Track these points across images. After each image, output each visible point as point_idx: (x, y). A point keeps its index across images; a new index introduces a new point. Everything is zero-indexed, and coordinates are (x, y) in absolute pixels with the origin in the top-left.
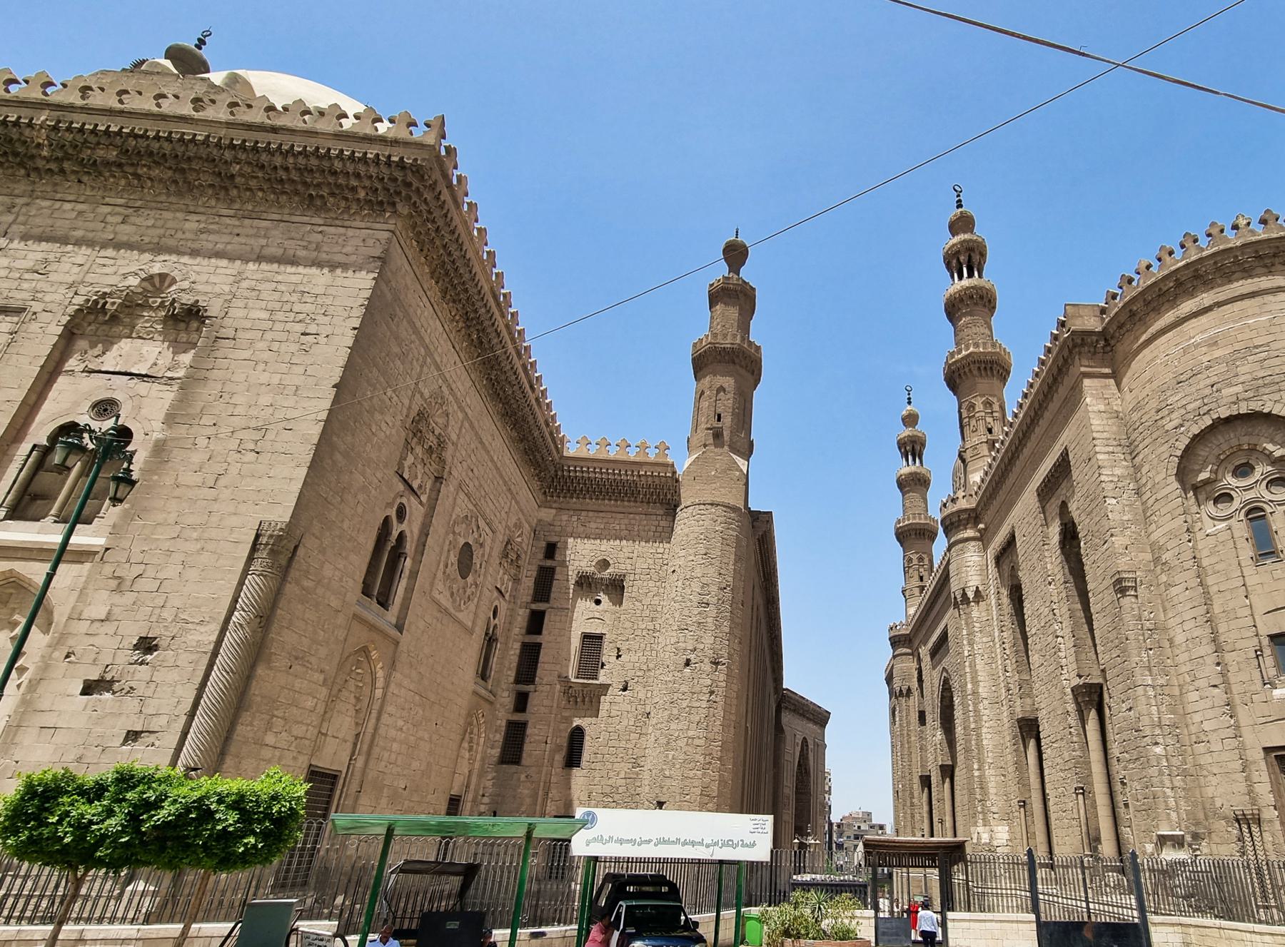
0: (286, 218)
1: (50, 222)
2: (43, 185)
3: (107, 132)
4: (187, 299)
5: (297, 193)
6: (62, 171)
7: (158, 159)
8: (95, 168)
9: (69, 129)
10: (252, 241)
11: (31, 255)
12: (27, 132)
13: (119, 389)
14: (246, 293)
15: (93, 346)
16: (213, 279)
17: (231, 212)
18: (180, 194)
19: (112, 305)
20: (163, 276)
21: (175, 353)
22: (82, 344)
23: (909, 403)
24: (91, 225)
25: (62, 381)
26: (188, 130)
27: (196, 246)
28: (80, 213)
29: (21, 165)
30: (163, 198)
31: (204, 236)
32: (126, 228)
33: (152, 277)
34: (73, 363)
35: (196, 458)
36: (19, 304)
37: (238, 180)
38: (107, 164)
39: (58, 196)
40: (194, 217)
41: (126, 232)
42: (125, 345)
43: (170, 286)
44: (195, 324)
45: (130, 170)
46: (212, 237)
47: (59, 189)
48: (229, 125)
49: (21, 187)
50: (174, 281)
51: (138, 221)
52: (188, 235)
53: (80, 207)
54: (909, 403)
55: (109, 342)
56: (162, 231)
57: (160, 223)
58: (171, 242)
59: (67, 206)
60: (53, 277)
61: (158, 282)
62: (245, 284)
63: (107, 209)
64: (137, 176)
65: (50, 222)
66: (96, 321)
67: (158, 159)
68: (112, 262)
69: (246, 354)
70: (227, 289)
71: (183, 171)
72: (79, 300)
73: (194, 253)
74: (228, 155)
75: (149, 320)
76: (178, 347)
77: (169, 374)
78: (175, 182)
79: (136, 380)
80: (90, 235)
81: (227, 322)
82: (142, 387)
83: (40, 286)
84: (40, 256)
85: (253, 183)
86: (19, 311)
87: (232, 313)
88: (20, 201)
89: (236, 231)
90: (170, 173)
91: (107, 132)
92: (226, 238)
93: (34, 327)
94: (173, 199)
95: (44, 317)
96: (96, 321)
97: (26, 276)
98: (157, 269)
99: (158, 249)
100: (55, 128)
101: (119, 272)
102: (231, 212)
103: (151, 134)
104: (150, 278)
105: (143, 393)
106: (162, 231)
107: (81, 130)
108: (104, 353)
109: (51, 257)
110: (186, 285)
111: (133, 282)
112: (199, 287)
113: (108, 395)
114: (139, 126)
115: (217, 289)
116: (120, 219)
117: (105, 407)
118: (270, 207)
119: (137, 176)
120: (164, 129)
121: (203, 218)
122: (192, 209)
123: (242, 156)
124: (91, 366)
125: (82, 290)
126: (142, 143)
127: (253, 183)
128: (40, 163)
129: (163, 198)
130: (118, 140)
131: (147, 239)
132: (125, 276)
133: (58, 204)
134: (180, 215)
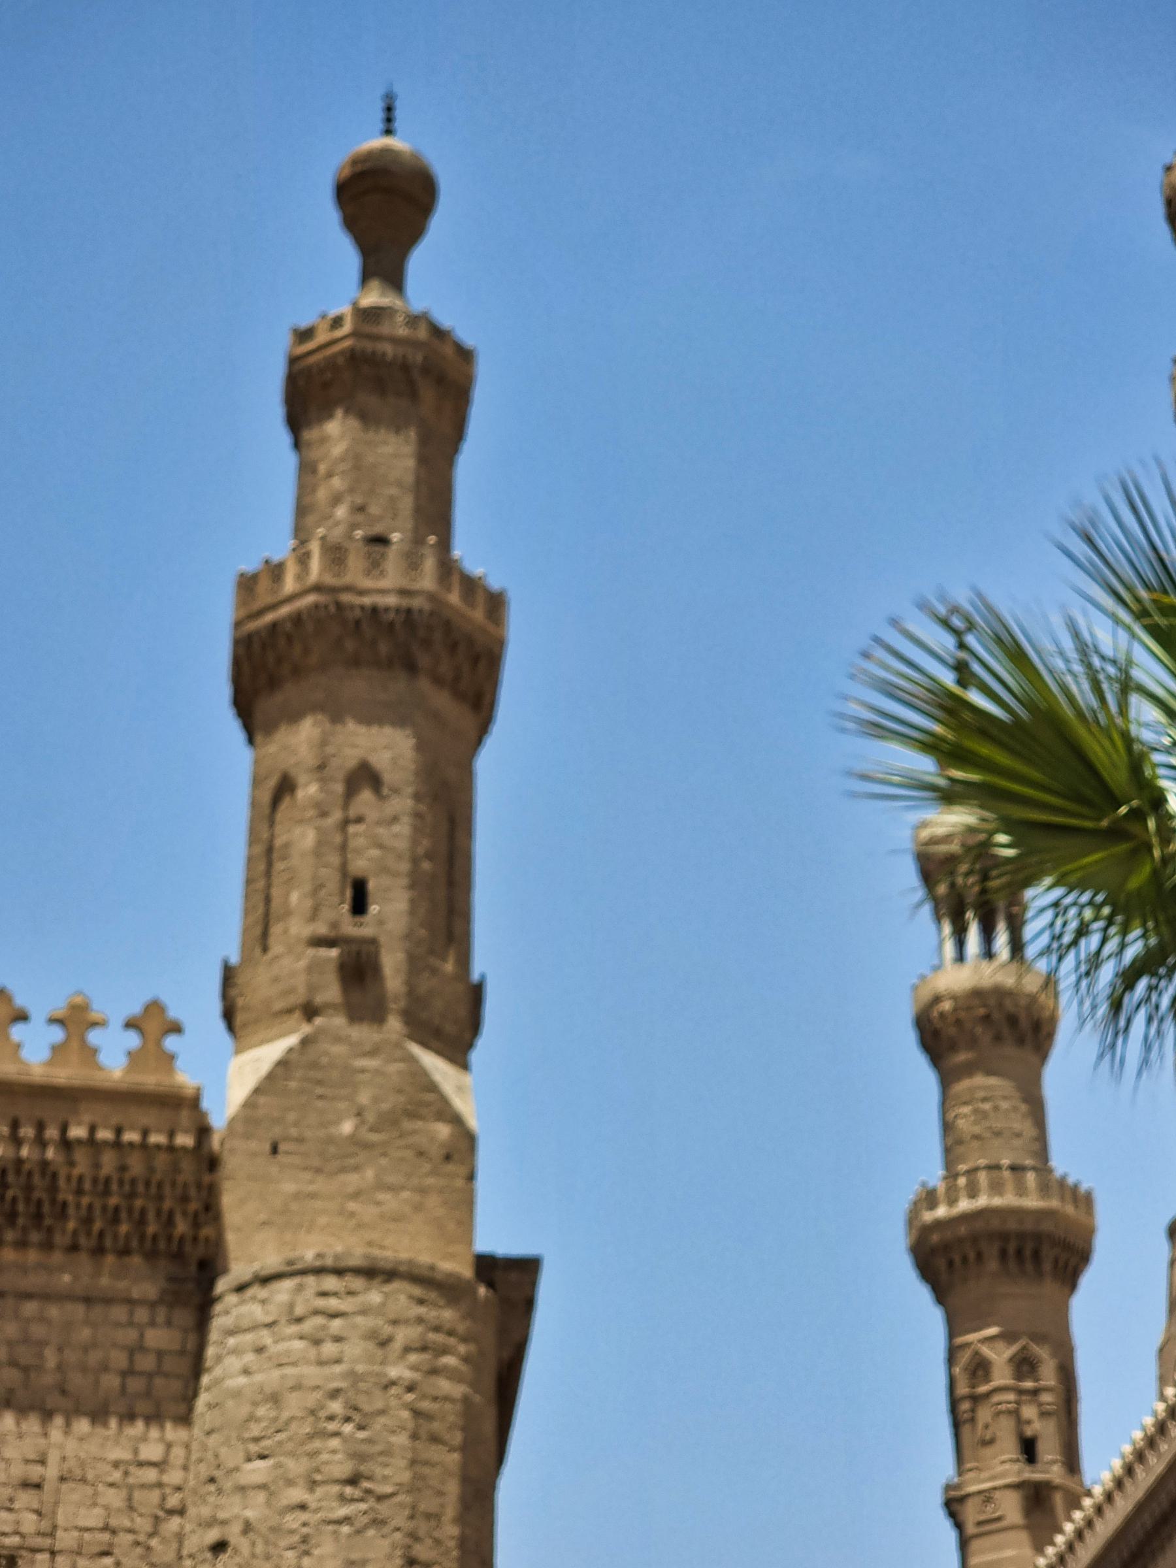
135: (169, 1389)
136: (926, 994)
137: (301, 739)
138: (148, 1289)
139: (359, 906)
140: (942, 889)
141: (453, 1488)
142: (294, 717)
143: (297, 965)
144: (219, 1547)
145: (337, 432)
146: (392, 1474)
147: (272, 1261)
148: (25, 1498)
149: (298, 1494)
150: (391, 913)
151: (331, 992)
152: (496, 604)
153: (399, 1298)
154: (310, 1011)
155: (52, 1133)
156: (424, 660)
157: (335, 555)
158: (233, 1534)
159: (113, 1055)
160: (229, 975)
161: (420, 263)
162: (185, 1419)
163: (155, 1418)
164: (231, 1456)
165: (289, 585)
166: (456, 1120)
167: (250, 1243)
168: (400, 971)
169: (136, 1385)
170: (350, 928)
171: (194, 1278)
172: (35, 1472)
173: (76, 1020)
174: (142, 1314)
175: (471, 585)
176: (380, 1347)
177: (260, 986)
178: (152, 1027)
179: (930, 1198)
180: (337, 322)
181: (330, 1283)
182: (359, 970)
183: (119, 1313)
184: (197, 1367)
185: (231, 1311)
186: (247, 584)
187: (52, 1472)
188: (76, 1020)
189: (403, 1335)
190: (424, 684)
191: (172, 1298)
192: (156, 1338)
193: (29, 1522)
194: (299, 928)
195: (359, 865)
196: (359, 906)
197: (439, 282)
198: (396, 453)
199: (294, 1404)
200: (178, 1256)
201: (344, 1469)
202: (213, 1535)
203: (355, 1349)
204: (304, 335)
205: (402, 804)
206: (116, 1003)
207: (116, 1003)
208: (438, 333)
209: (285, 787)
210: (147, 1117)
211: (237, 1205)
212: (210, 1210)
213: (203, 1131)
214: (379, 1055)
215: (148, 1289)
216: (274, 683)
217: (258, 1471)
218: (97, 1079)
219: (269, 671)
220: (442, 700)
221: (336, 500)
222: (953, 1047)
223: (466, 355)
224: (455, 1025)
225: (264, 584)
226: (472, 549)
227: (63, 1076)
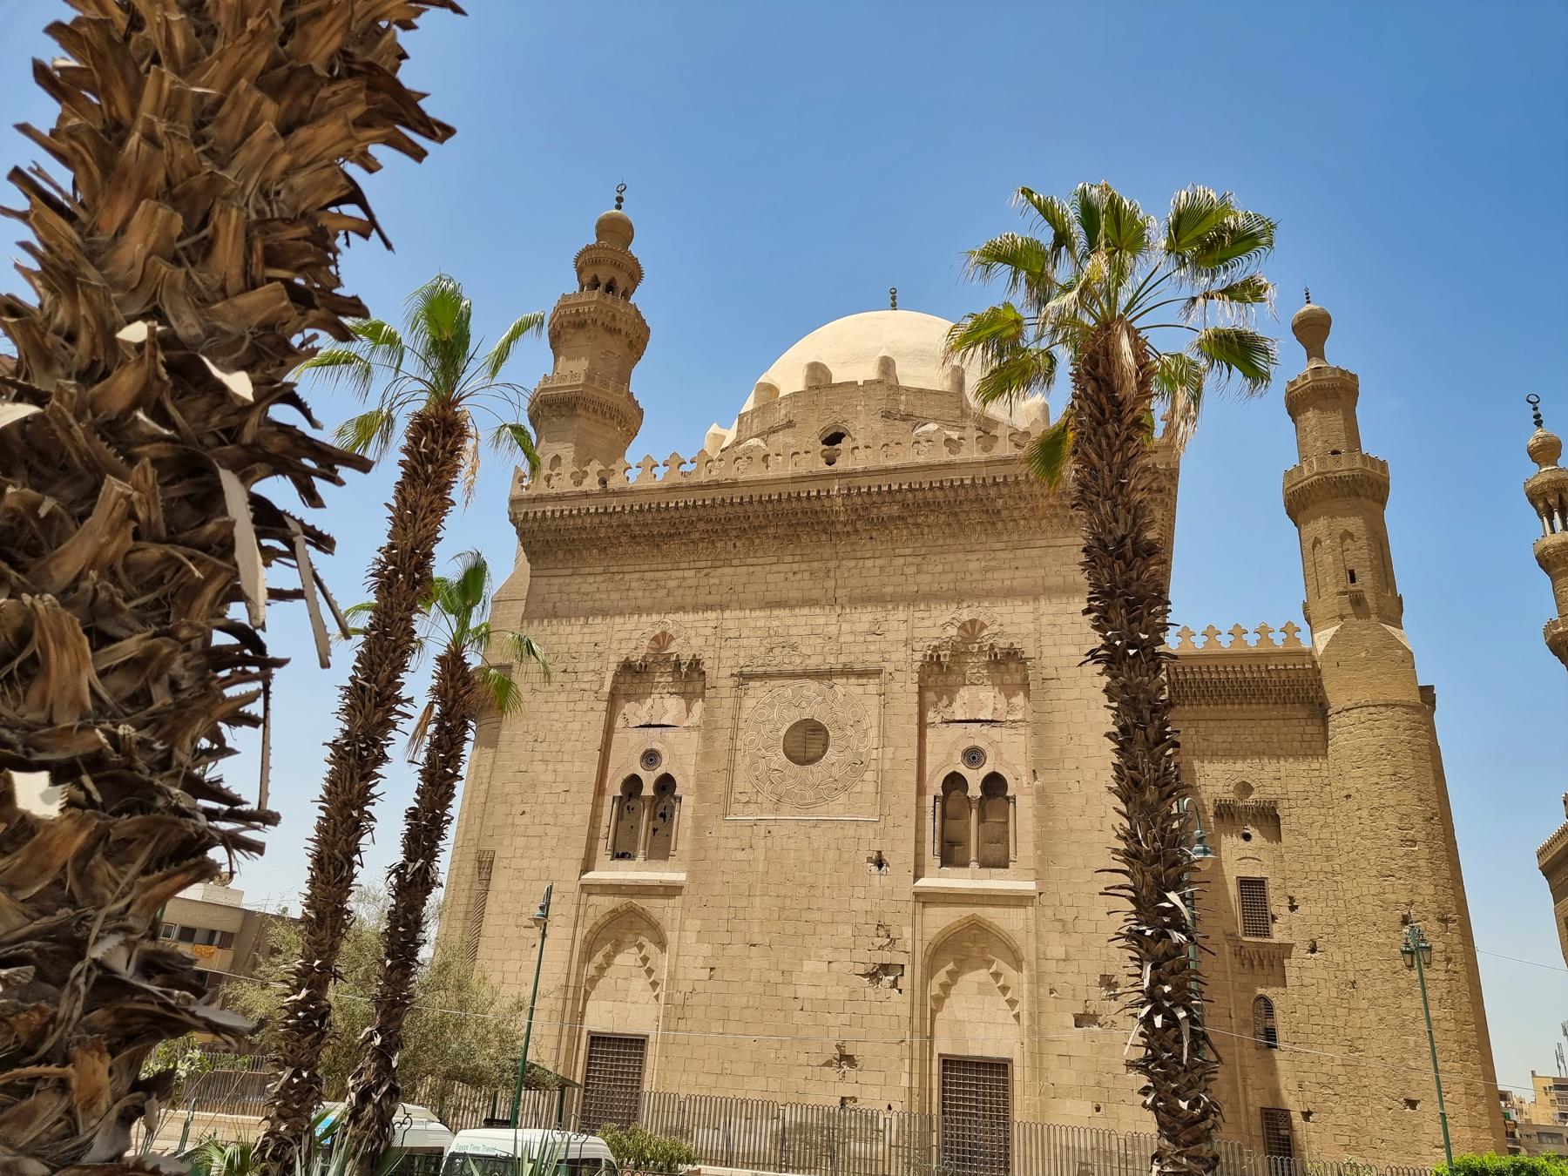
0: (1052, 542)
1: (862, 581)
2: (841, 548)
3: (890, 491)
4: (1003, 643)
5: (1056, 515)
6: (856, 531)
7: (932, 507)
8: (882, 523)
9: (859, 494)
10: (1031, 573)
11: (863, 618)
12: (827, 502)
13: (978, 736)
14: (1050, 629)
15: (940, 699)
16: (1016, 619)
17: (1002, 545)
18: (954, 535)
19: (945, 655)
20: (973, 622)
21: (1008, 697)
22: (930, 696)
23: (1539, 423)
24: (895, 579)
25: (929, 732)
26: (955, 476)
27: (987, 586)
28: (882, 568)
29: (825, 531)
30: (941, 542)
31: (989, 575)
32: (924, 578)
33: (964, 624)
34: (931, 716)
35: (1076, 802)
36: (873, 667)
37: (1005, 513)
38: (892, 518)
39: (858, 555)
40: (974, 557)
41: (925, 582)
42: (964, 694)
43: (981, 630)
44: (1013, 665)
45: (910, 520)
46: (996, 575)
47: (857, 547)
48: (988, 463)
49: (827, 551)
50: (983, 626)
51: (930, 568)
52: (977, 576)
53: (879, 562)
54: (1539, 423)
55: (949, 692)
56: (951, 576)
57: (948, 567)
58: (966, 586)
59: (869, 563)
60: (889, 636)
61: (971, 629)
62: (1044, 620)
63: (901, 561)
64: (917, 525)
65: (862, 581)
66: (938, 674)
67: (932, 507)
68: (926, 614)
69: (1074, 693)
70: (1031, 627)
71: (956, 514)
72: (918, 656)
73: (990, 594)
74: (993, 492)
75: (974, 666)
76: (1008, 691)
77: (1010, 718)
78: (949, 525)
79: (986, 727)
80: (899, 589)
81: (1045, 662)
82: (995, 733)
83: (883, 646)
84: (870, 617)
85: (1016, 514)
86: (878, 672)
87: (1045, 650)
88: (832, 564)
89: (1014, 564)
90: (943, 518)
91: (890, 491)
92: (1007, 574)
93: (896, 687)
94: (949, 541)
95: (897, 675)
96: (938, 674)
97: (869, 638)
98: (966, 615)
99: (959, 597)
100: (849, 495)
101: (938, 625)
102: (1002, 545)
103: (926, 486)
104: (963, 627)
105: (998, 738)
106: (951, 576)
107: (869, 493)
108: (951, 703)
109: (879, 616)
110: (995, 628)
111: (953, 631)
112: (1008, 629)
113: (969, 744)
114: (915, 479)
115: (1023, 630)
116: (913, 569)
117: (974, 756)
118: (1034, 533)
119: (917, 525)
120: (936, 477)
121: (981, 556)
122: (968, 548)
123: (1005, 491)
124: (947, 717)
125: (917, 646)
126: (919, 495)
127: (1016, 514)
128: (839, 527)
129: (941, 542)
130: (899, 497)
131: (945, 586)
132: (944, 627)
133: (861, 563)
134: (960, 556)
135: (1318, 746)
136: (1540, 547)
137: (1320, 526)
138: (1303, 714)
139: (1353, 580)
140: (1541, 505)
141: (1431, 774)
142: (1316, 518)
143: (1331, 600)
144: (1348, 796)
145: (1311, 416)
146: (1407, 771)
147: (1349, 704)
148: (1275, 783)
149: (1375, 779)
150: (1366, 579)
151: (1349, 610)
152: (1383, 465)
153: (1399, 711)
154: (1342, 617)
155: (1263, 668)
156: (1361, 492)
157: (1321, 461)
158: (1353, 792)
159: (1278, 640)
160: (1306, 607)
161: (1328, 346)
162: (1326, 755)
163: (1315, 756)
164: (1347, 767)
165: (1306, 473)
166: (1404, 648)
167: (1336, 697)
168: (1370, 596)
169: (1305, 745)
170: (1351, 587)
171: (1320, 711)
172: (1278, 775)
173: (1263, 631)
174: (1303, 722)
175: (1374, 461)
176: (1390, 728)
177: (1318, 609)
178: (1290, 630)
179: (1555, 624)
180: (1305, 377)
181: (1372, 710)
182: (1357, 601)
183: (1295, 722)
184: (1326, 739)
185: (1334, 721)
186: (1288, 474)
187: (1283, 774)
188: (1263, 631)
189: (1402, 725)
190: (1363, 499)
191: (1312, 716)
192: (1309, 729)
193: (1279, 791)
194: (1332, 589)
195: (1350, 566)
196: (1353, 580)
197: (1338, 353)
198: (1336, 420)
199: (1367, 750)
200: (1312, 703)
201: (1391, 771)
202: (1345, 793)
203: (1386, 731)
204: (1294, 383)
205: (1363, 542)
206: (1276, 624)
207: (1276, 624)
208: (1344, 372)
209: (1317, 542)
210: (1294, 660)
211: (1328, 686)
212: (1321, 686)
213: (1314, 662)
214: (1369, 630)
215: (1303, 714)
216: (1305, 507)
217: (1358, 773)
218: (1275, 650)
219: (1300, 503)
220: (1370, 503)
221: (1316, 440)
222: (1556, 566)
223: (1354, 377)
224: (1393, 612)
225: (1296, 474)
226: (1370, 445)
227: (1262, 650)
